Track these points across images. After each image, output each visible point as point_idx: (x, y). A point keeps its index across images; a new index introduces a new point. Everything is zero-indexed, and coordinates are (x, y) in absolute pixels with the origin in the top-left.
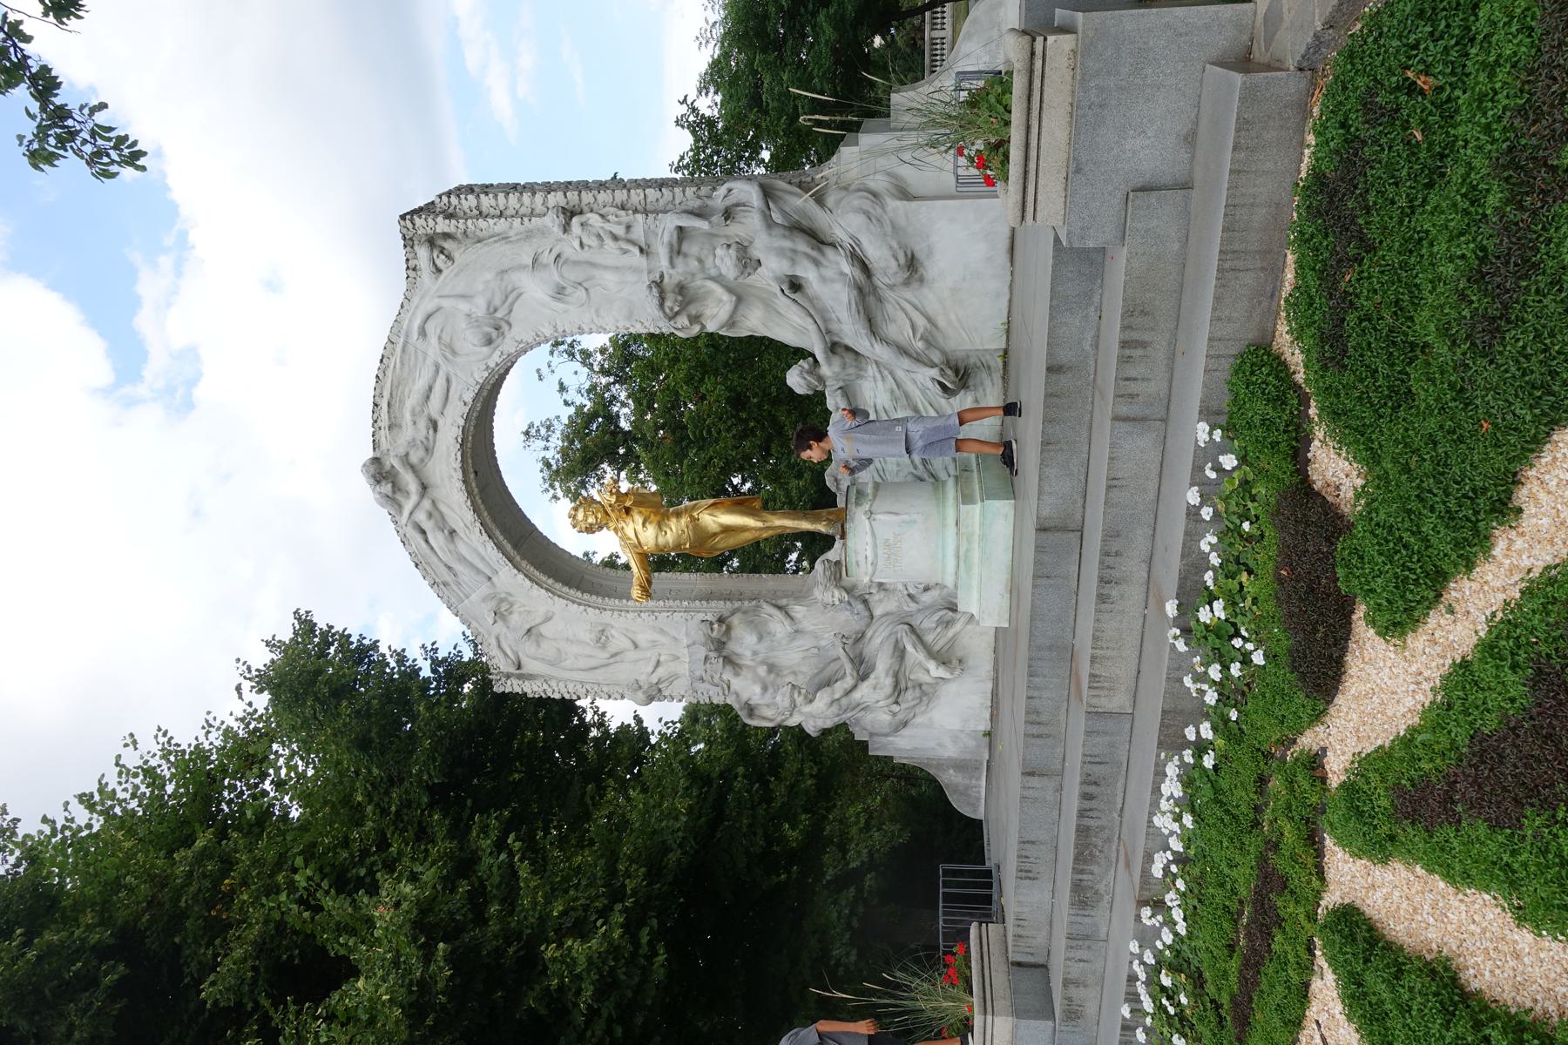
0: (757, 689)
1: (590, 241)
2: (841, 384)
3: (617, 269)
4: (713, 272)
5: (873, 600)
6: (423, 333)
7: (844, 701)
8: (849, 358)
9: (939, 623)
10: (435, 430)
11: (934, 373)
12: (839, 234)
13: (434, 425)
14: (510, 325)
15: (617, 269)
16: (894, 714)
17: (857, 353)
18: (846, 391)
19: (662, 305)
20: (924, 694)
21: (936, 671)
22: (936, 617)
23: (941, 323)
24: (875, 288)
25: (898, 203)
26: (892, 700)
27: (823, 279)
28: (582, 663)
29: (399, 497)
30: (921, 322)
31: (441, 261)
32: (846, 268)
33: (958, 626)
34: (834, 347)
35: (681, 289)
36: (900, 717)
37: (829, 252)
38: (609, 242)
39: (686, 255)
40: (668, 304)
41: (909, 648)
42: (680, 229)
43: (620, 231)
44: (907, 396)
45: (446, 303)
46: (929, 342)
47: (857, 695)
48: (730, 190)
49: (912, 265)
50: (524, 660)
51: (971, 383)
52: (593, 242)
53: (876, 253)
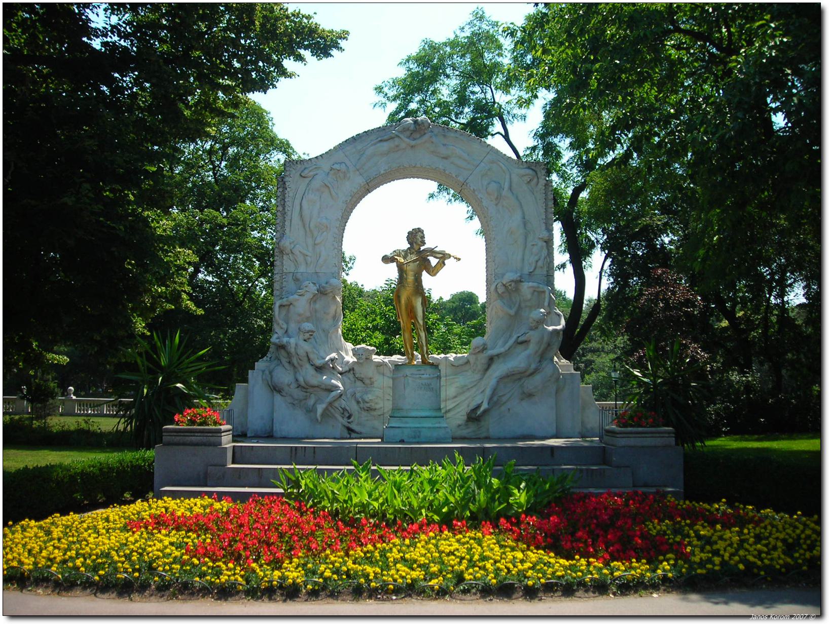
0: (301, 311)
1: (535, 249)
2: (472, 361)
3: (523, 259)
4: (523, 305)
5: (351, 375)
6: (493, 162)
7: (306, 359)
8: (486, 366)
9: (344, 410)
10: (443, 158)
11: (485, 406)
12: (544, 364)
13: (446, 158)
14: (496, 205)
15: (523, 259)
16: (289, 385)
17: (487, 369)
18: (468, 362)
19: (512, 281)
20: (301, 401)
21: (320, 409)
22: (348, 408)
23: (503, 408)
24: (520, 379)
25: (555, 388)
26: (303, 383)
27: (528, 357)
28: (306, 212)
29: (408, 133)
30: (504, 399)
31: (527, 179)
32: (533, 366)
33: (340, 419)
34: (491, 360)
35: (517, 290)
36: (286, 388)
37: (538, 359)
38: (536, 258)
39: (533, 294)
40: (513, 284)
41: (334, 394)
42: (544, 292)
43: (540, 263)
44: (464, 392)
45: (508, 176)
46: (496, 403)
47: (308, 366)
48: (559, 315)
49: (530, 395)
50: (307, 180)
51: (470, 423)
52: (535, 249)
53: (538, 378)
